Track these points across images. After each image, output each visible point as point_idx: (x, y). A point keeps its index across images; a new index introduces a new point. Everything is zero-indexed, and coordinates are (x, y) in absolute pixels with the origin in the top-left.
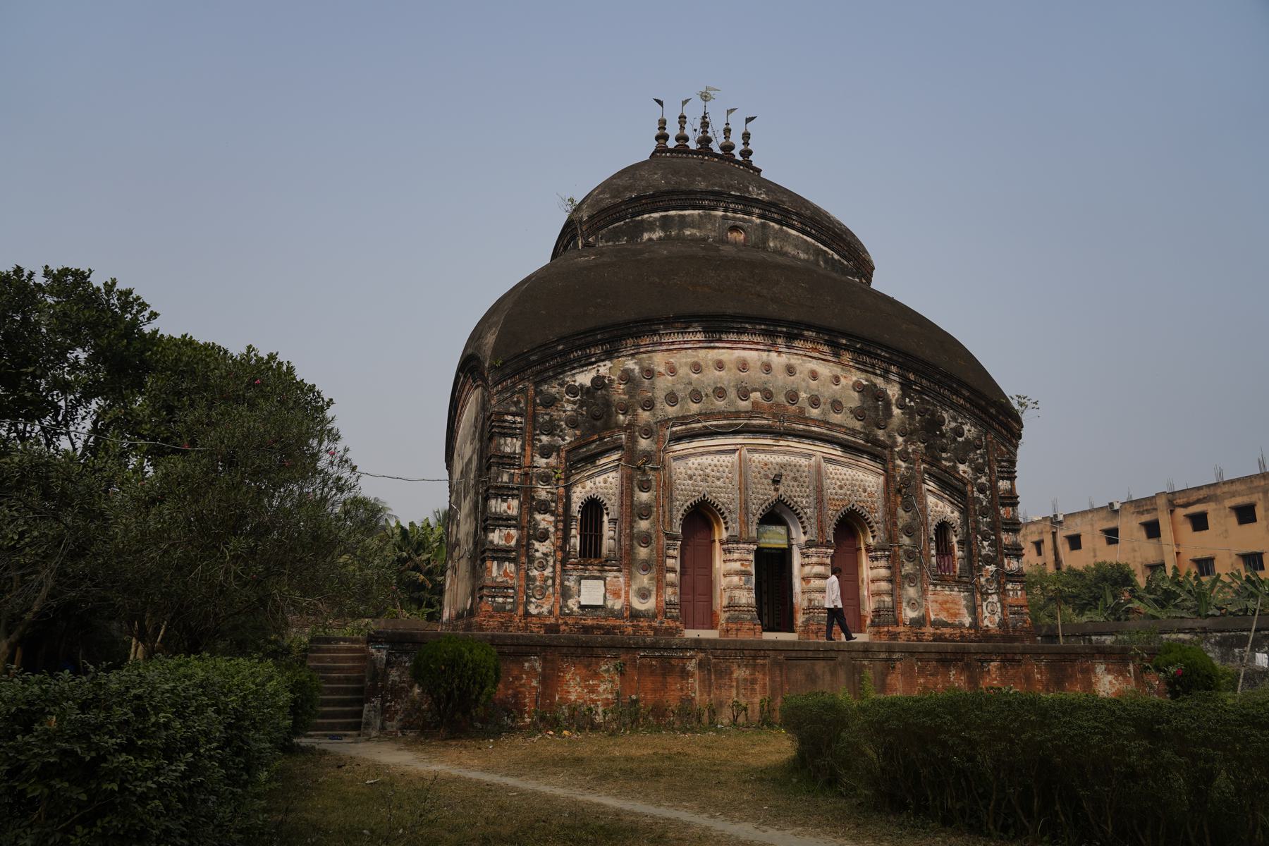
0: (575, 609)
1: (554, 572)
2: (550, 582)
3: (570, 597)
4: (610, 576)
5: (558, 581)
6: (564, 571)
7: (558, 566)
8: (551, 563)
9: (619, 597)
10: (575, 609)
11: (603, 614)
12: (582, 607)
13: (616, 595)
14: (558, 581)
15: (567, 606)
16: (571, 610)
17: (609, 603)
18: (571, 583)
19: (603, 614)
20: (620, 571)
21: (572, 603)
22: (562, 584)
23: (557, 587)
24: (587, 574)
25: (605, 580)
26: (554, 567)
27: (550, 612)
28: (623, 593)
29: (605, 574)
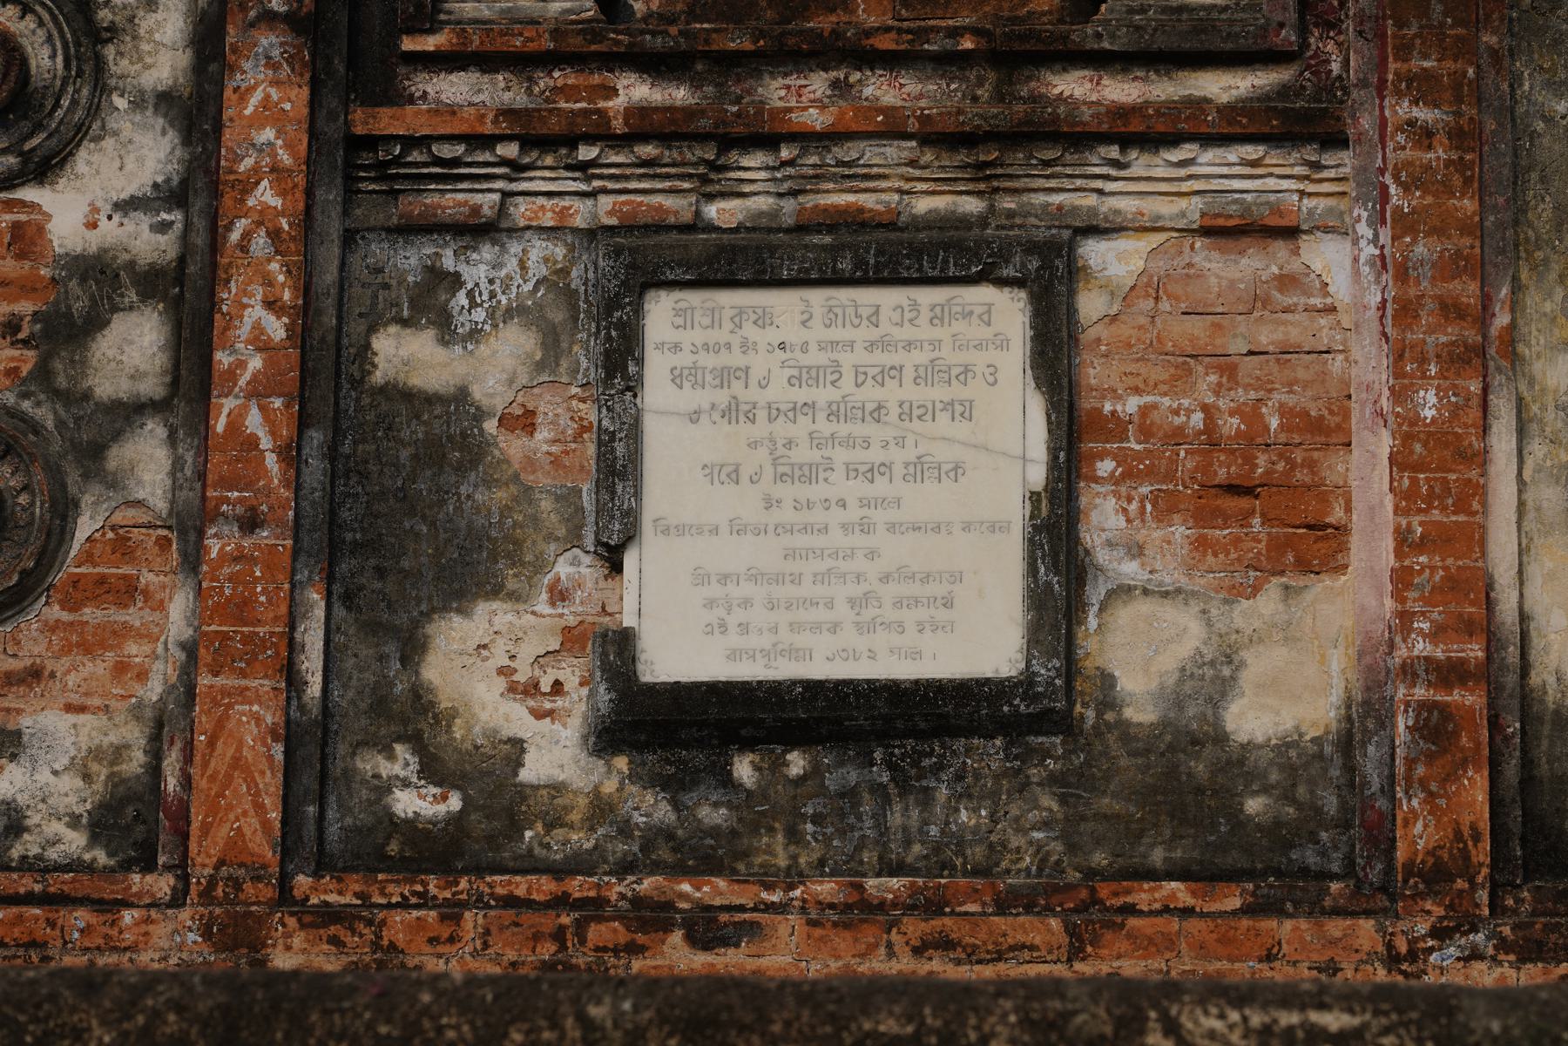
0: (556, 755)
1: (200, 188)
2: (133, 348)
3: (473, 568)
4: (1138, 228)
5: (255, 322)
6: (357, 169)
7: (268, 106)
8: (160, 51)
9: (1313, 544)
10: (556, 755)
11: (1030, 830)
12: (663, 726)
13: (1263, 508)
14: (255, 322)
15: (414, 719)
16: (490, 776)
17: (1142, 654)
18: (477, 356)
19: (1030, 830)
20: (1303, 124)
21: (496, 672)
22: (324, 367)
23: (251, 417)
24: (751, 196)
25: (1046, 272)
26: (197, 112)
27: (135, 821)
28: (1367, 475)
29: (1056, 195)
